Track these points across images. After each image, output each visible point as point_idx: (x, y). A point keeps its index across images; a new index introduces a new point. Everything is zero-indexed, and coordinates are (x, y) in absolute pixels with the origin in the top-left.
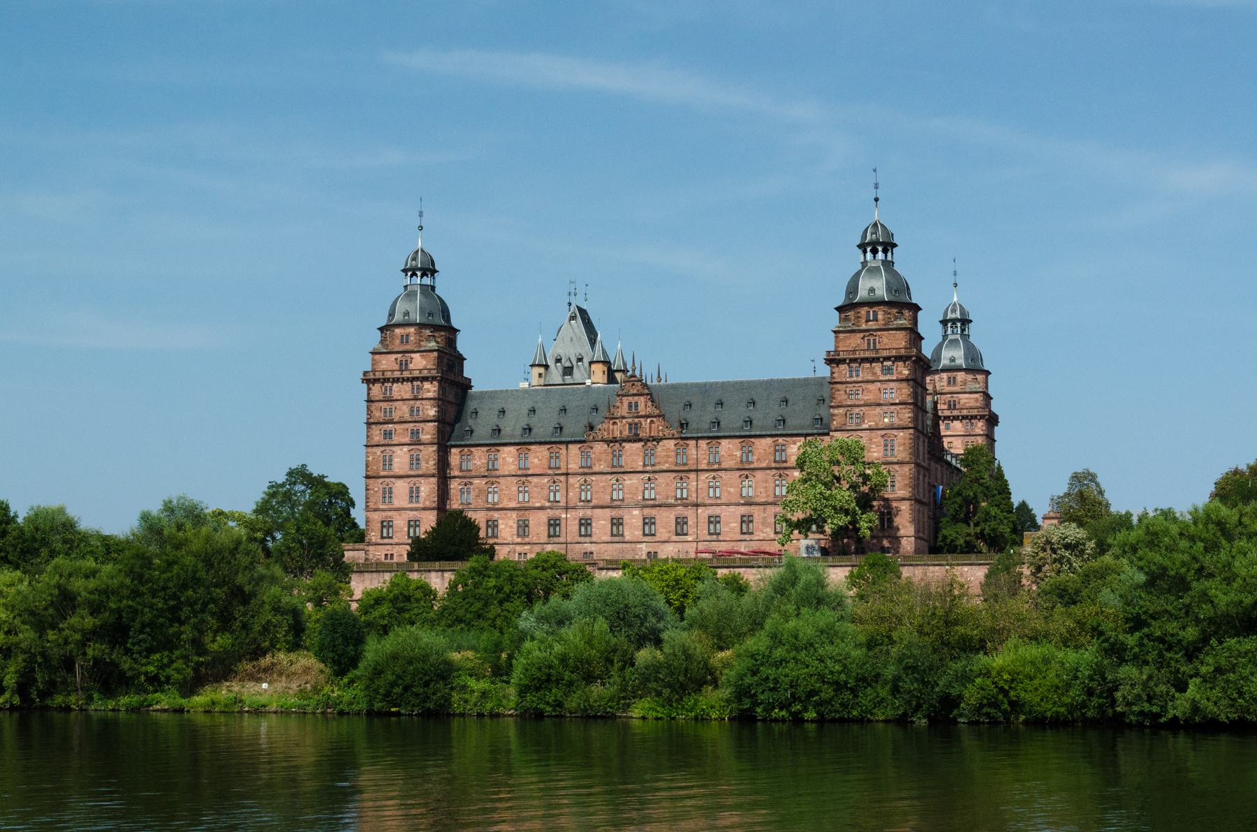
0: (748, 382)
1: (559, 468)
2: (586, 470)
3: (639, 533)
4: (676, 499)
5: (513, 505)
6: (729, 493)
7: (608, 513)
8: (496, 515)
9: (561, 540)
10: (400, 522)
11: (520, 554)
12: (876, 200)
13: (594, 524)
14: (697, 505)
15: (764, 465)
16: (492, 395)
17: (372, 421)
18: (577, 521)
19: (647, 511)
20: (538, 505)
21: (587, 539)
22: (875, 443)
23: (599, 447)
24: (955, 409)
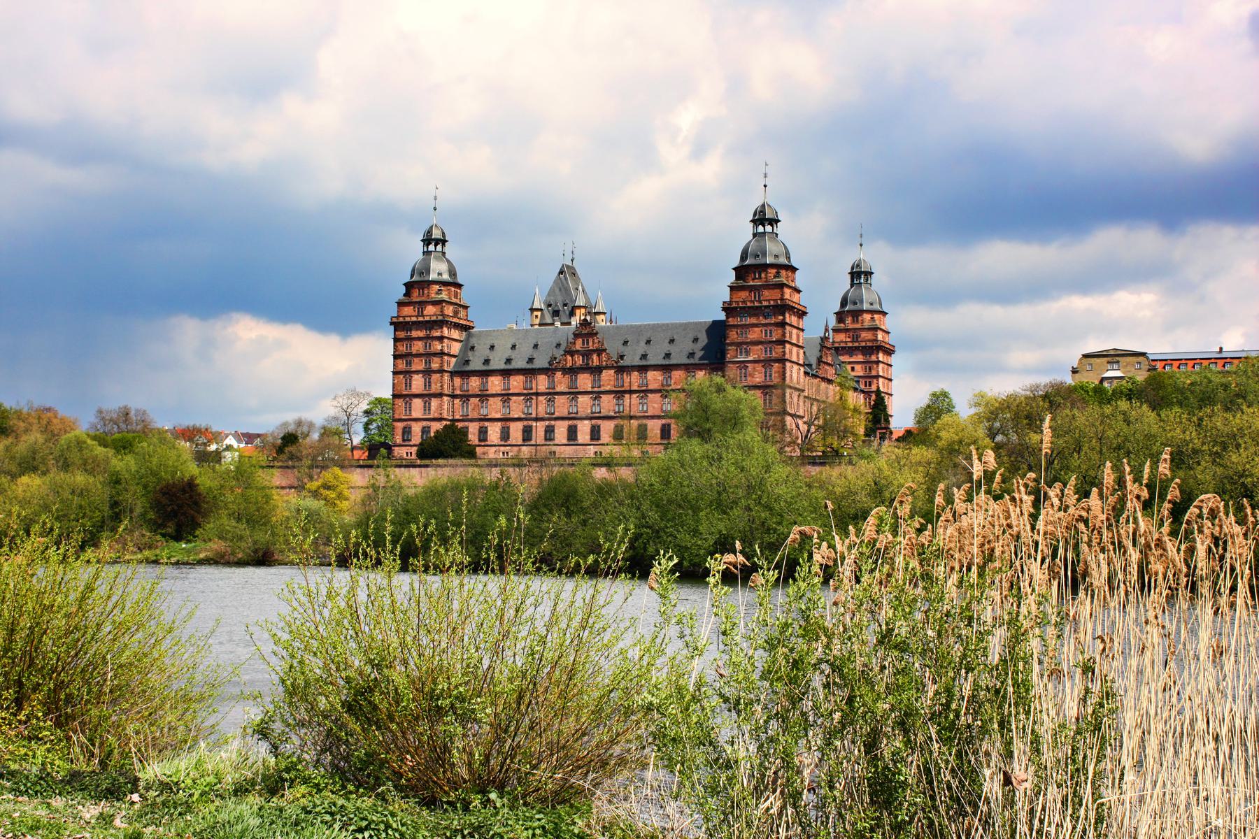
0: (672, 324)
1: (531, 389)
2: (551, 391)
3: (588, 437)
4: (615, 413)
5: (498, 416)
6: (654, 407)
7: (566, 423)
8: (486, 424)
9: (533, 442)
10: (416, 428)
11: (503, 453)
12: (765, 186)
13: (556, 431)
14: (631, 417)
15: (679, 387)
16: (488, 334)
17: (397, 353)
18: (544, 429)
19: (594, 422)
20: (516, 416)
21: (551, 443)
22: (757, 371)
23: (559, 374)
24: (857, 341)
